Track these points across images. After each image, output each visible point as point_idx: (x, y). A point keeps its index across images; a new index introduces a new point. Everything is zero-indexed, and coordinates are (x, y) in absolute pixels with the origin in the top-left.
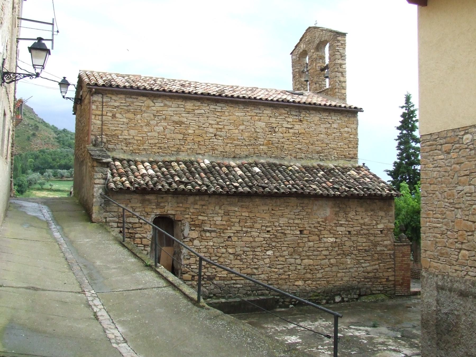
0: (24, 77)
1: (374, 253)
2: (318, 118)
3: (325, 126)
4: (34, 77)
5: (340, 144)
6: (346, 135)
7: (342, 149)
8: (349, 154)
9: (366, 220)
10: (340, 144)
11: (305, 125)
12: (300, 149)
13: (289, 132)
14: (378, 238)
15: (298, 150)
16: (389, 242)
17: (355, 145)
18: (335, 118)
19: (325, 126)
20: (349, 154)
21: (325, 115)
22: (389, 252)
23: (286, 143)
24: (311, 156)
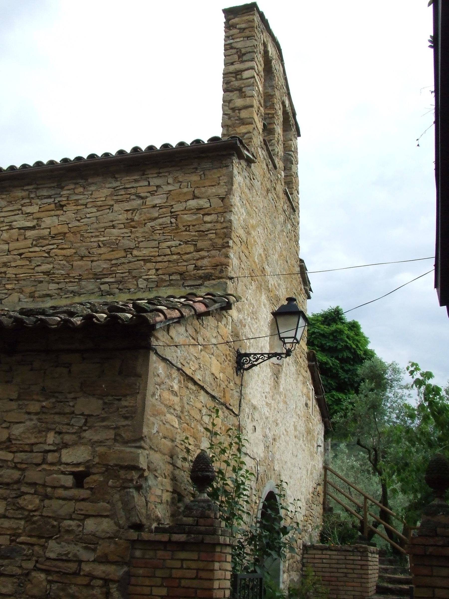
0: (269, 358)
1: (30, 565)
2: (106, 192)
3: (127, 206)
4: (284, 356)
5: (169, 244)
6: (188, 218)
7: (175, 257)
8: (197, 268)
9: (17, 430)
10: (169, 244)
11: (69, 214)
12: (47, 273)
13: (25, 239)
14: (55, 504)
15: (41, 277)
16: (106, 526)
17: (219, 242)
18: (157, 181)
19: (127, 206)
20: (197, 268)
21: (128, 181)
22: (100, 570)
23: (13, 264)
24: (75, 288)
